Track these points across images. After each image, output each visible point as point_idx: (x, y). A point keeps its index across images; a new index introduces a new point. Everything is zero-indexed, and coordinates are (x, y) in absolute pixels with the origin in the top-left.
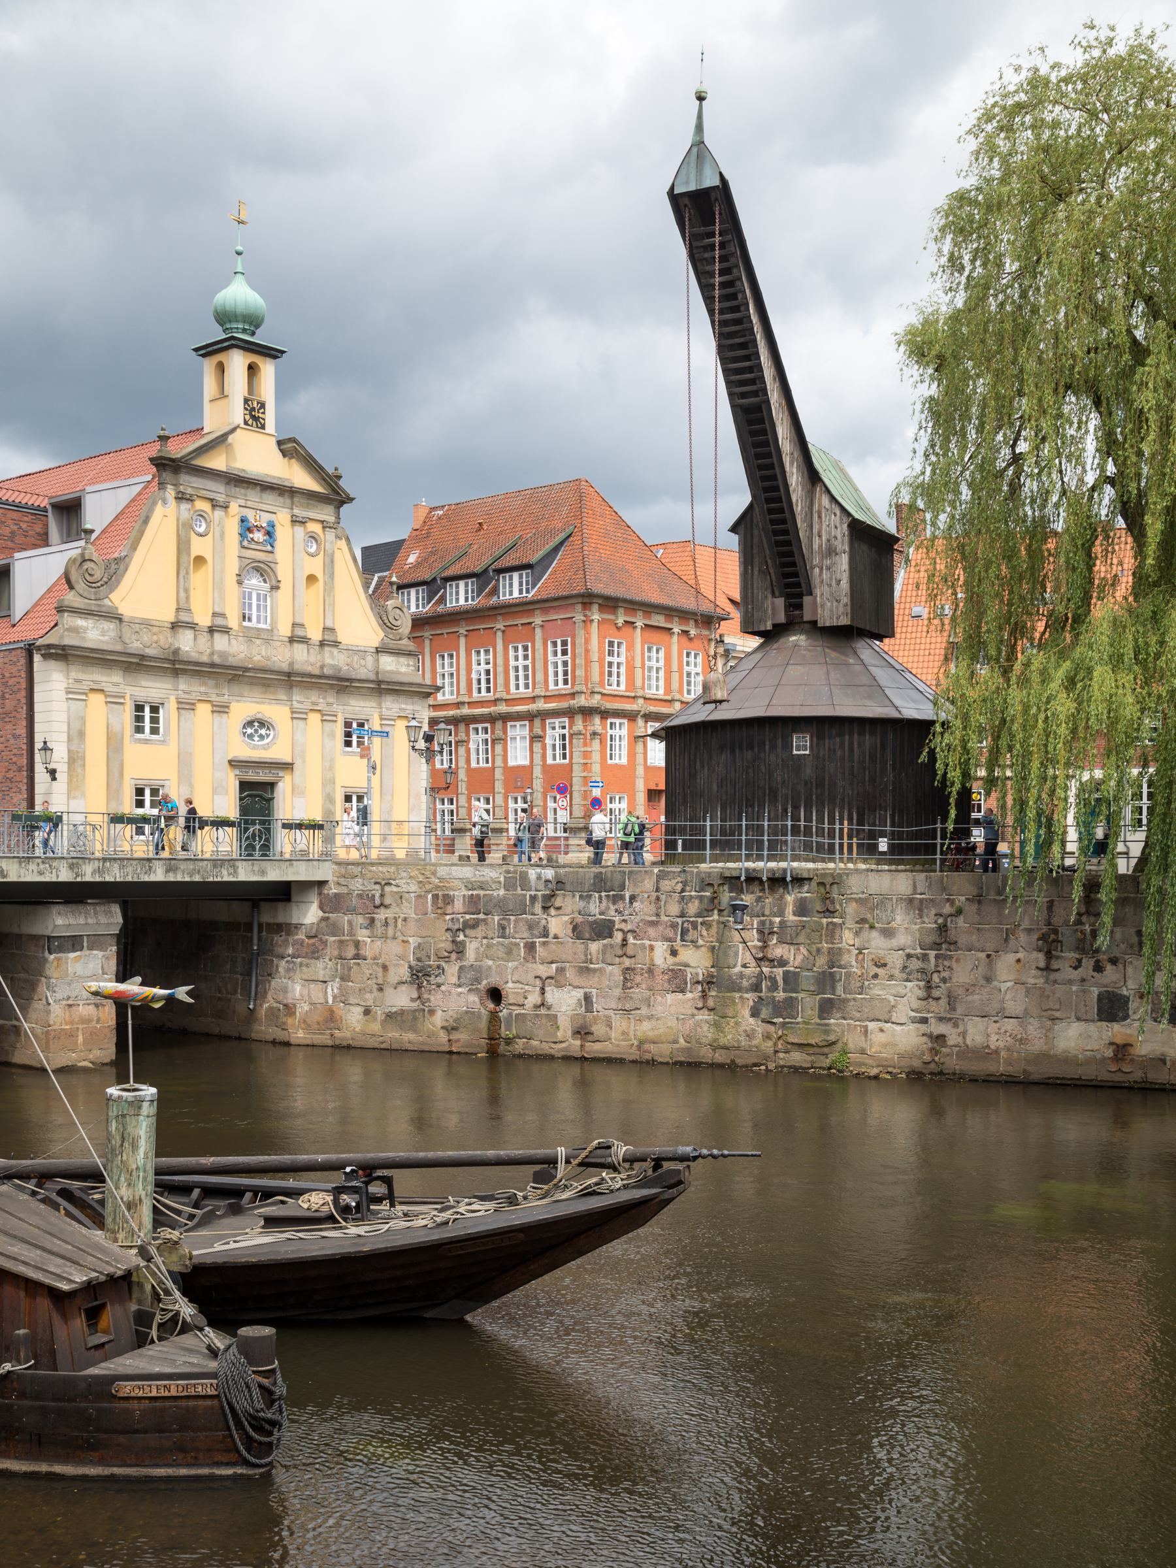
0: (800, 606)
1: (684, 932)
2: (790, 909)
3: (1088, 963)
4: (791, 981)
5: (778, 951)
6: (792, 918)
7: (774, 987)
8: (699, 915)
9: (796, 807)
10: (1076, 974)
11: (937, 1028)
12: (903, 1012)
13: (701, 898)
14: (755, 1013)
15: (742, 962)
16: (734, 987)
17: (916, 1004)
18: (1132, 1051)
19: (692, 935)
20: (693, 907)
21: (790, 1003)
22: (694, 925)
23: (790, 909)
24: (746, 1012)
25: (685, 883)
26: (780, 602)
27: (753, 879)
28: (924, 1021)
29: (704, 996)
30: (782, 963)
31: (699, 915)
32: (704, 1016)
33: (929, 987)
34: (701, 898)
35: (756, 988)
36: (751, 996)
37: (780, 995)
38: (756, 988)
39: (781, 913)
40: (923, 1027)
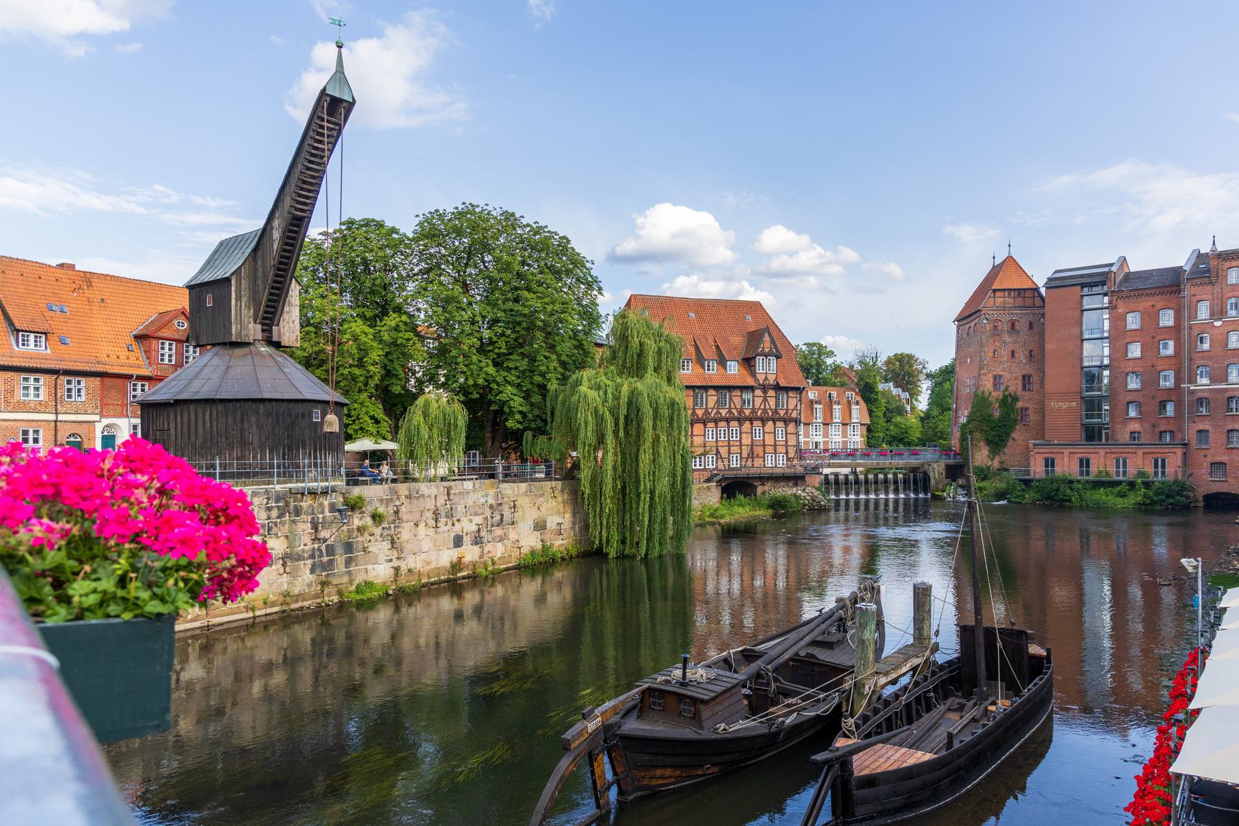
0: (270, 331)
1: (270, 529)
2: (327, 510)
3: (450, 523)
4: (331, 550)
5: (324, 534)
6: (327, 514)
7: (321, 555)
8: (278, 517)
9: (315, 452)
10: (446, 528)
11: (395, 563)
12: (382, 558)
13: (278, 507)
14: (312, 571)
15: (305, 542)
16: (300, 558)
17: (388, 553)
18: (464, 560)
19: (275, 530)
20: (274, 513)
21: (331, 562)
22: (276, 524)
23: (327, 510)
24: (308, 572)
25: (268, 499)
26: (259, 327)
27: (313, 493)
28: (391, 560)
29: (284, 565)
30: (325, 540)
31: (278, 517)
32: (285, 578)
33: (393, 542)
34: (278, 507)
35: (312, 556)
36: (309, 562)
37: (325, 559)
38: (312, 556)
39: (323, 512)
40: (391, 564)
